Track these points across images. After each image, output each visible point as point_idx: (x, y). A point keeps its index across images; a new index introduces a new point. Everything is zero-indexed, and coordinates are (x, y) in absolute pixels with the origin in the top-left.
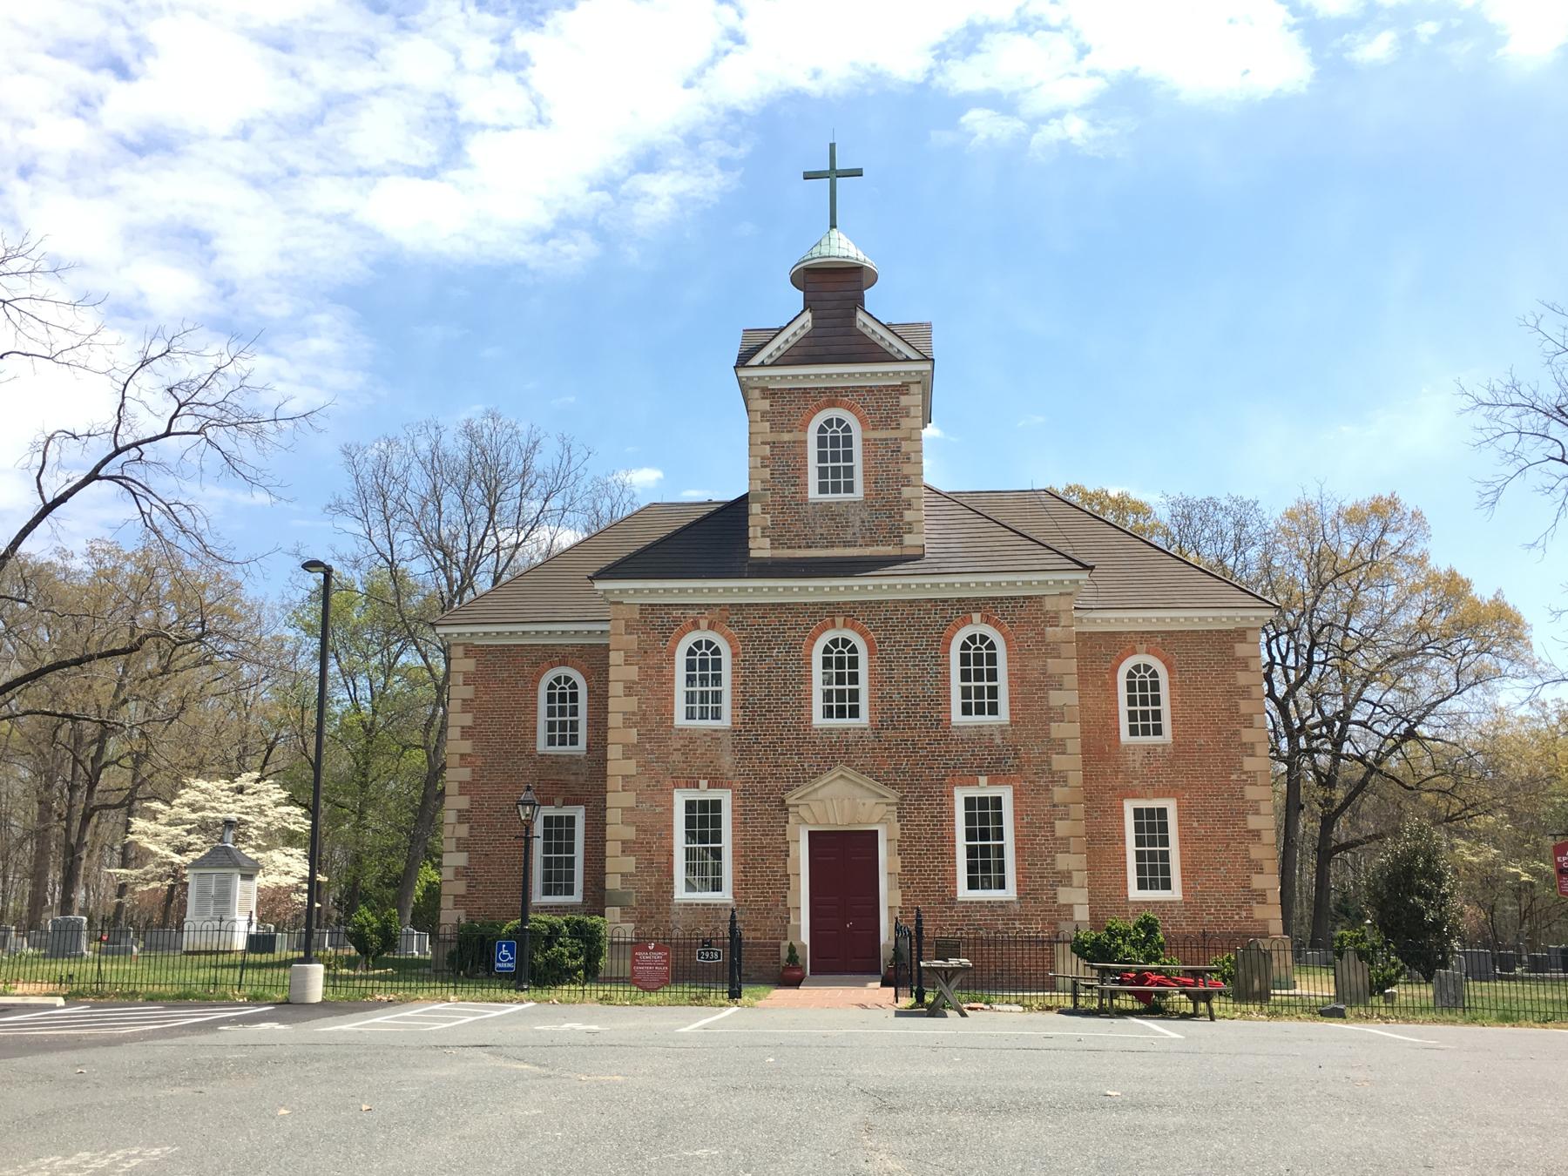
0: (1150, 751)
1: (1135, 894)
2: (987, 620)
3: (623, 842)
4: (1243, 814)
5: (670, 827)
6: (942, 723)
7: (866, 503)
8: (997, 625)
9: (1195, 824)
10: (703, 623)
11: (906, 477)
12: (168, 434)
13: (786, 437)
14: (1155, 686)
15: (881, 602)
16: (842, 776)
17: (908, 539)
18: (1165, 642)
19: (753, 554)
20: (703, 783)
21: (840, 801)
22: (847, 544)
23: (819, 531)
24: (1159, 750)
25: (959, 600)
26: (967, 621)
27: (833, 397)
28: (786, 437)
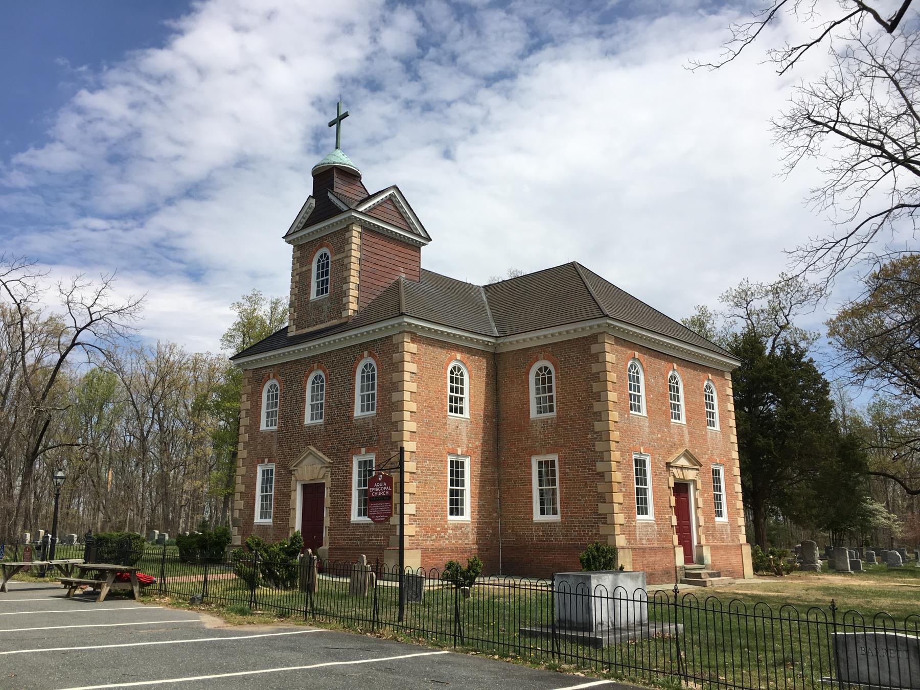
0: (544, 422)
1: (537, 517)
2: (370, 355)
3: (241, 493)
4: (594, 462)
5: (255, 484)
6: (350, 417)
7: (330, 298)
8: (374, 357)
9: (568, 470)
10: (271, 375)
11: (345, 278)
12: (92, 321)
13: (304, 269)
14: (550, 379)
15: (331, 352)
16: (310, 453)
17: (344, 314)
18: (553, 350)
19: (289, 335)
20: (266, 460)
21: (311, 468)
22: (322, 322)
23: (313, 317)
24: (549, 421)
25: (360, 344)
26: (362, 357)
27: (320, 242)
28: (304, 269)
